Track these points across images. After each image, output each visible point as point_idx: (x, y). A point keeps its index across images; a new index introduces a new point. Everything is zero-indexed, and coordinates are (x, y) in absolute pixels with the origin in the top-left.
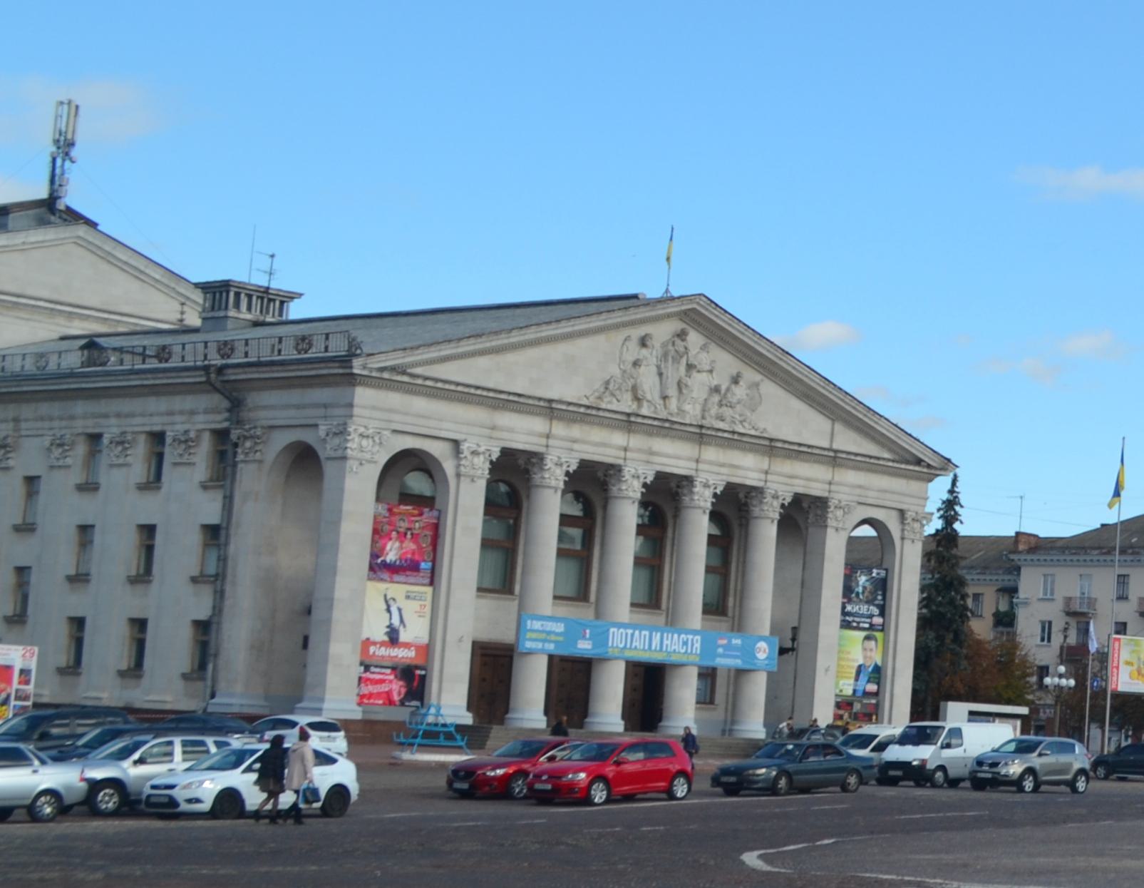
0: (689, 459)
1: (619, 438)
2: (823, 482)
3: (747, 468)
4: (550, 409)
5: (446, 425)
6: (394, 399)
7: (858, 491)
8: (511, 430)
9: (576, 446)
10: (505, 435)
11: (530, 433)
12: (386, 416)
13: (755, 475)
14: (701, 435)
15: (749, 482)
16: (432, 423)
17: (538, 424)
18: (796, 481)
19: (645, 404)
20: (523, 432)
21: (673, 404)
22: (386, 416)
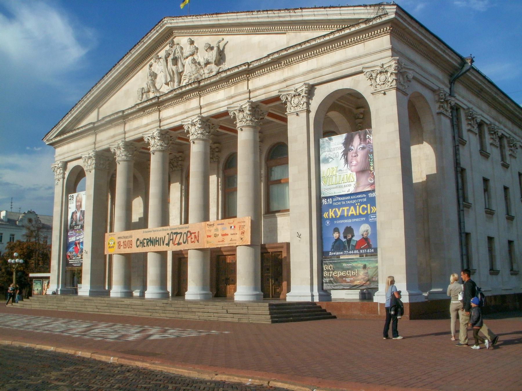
0: (182, 113)
14: (181, 96)
16: (76, 152)
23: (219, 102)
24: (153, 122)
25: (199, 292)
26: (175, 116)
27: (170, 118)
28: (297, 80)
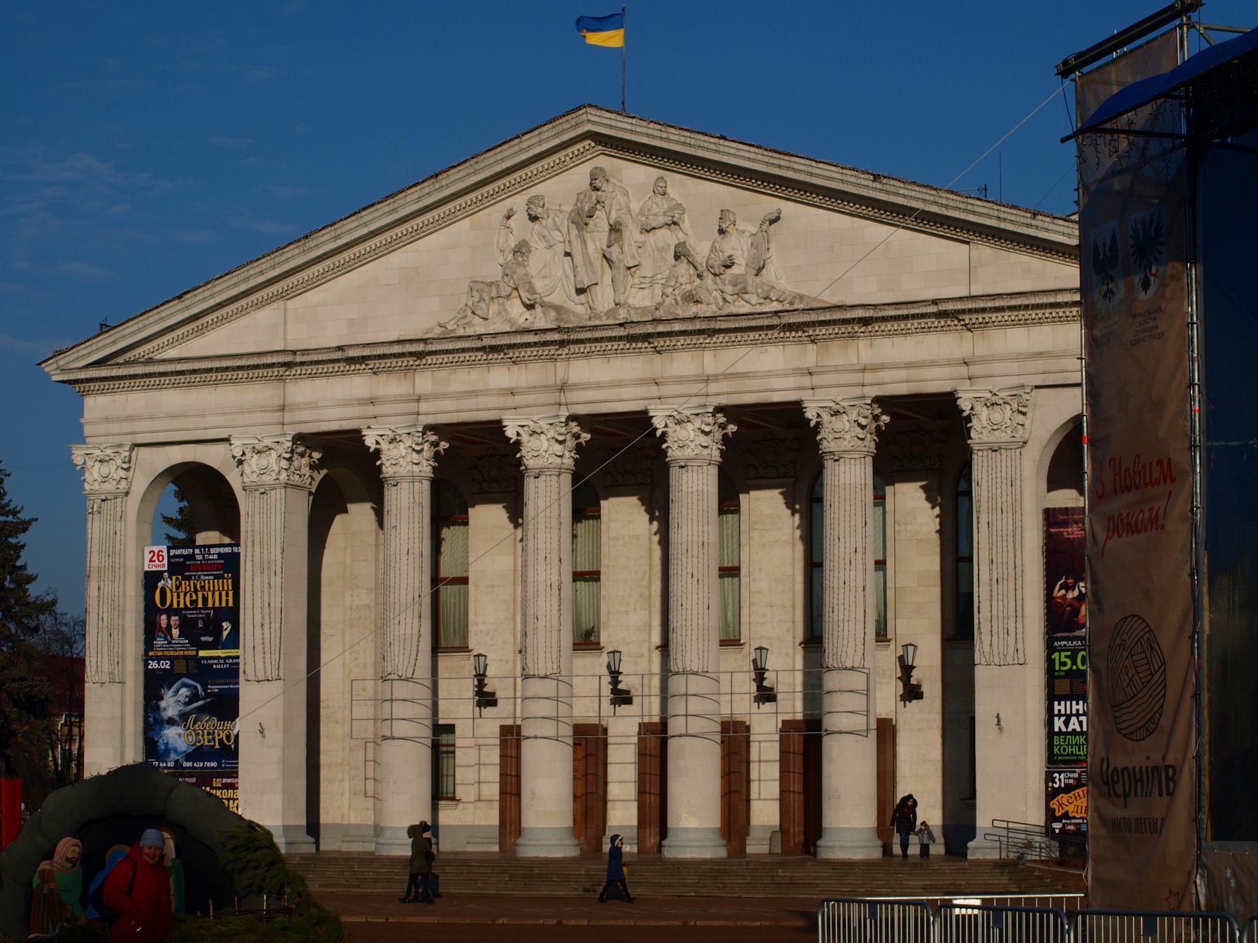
0: (642, 382)
1: (500, 376)
2: (950, 363)
3: (768, 372)
4: (350, 359)
5: (210, 421)
6: (135, 401)
7: (1040, 365)
8: (313, 405)
9: (424, 407)
10: (306, 415)
11: (345, 403)
12: (126, 427)
13: (791, 382)
15: (777, 397)
16: (190, 423)
17: (357, 385)
18: (886, 375)
19: (538, 309)
20: (329, 403)
21: (604, 299)
22: (126, 427)
23: (769, 375)
24: (535, 389)
25: (717, 842)
26: (618, 384)
27: (599, 386)
28: (999, 367)
